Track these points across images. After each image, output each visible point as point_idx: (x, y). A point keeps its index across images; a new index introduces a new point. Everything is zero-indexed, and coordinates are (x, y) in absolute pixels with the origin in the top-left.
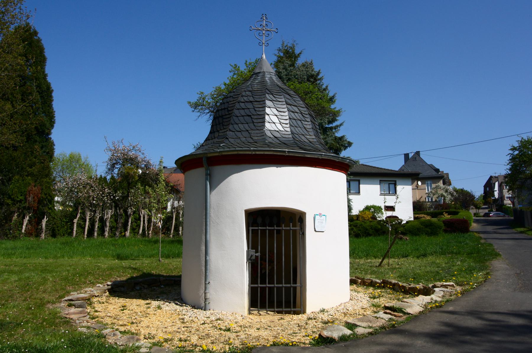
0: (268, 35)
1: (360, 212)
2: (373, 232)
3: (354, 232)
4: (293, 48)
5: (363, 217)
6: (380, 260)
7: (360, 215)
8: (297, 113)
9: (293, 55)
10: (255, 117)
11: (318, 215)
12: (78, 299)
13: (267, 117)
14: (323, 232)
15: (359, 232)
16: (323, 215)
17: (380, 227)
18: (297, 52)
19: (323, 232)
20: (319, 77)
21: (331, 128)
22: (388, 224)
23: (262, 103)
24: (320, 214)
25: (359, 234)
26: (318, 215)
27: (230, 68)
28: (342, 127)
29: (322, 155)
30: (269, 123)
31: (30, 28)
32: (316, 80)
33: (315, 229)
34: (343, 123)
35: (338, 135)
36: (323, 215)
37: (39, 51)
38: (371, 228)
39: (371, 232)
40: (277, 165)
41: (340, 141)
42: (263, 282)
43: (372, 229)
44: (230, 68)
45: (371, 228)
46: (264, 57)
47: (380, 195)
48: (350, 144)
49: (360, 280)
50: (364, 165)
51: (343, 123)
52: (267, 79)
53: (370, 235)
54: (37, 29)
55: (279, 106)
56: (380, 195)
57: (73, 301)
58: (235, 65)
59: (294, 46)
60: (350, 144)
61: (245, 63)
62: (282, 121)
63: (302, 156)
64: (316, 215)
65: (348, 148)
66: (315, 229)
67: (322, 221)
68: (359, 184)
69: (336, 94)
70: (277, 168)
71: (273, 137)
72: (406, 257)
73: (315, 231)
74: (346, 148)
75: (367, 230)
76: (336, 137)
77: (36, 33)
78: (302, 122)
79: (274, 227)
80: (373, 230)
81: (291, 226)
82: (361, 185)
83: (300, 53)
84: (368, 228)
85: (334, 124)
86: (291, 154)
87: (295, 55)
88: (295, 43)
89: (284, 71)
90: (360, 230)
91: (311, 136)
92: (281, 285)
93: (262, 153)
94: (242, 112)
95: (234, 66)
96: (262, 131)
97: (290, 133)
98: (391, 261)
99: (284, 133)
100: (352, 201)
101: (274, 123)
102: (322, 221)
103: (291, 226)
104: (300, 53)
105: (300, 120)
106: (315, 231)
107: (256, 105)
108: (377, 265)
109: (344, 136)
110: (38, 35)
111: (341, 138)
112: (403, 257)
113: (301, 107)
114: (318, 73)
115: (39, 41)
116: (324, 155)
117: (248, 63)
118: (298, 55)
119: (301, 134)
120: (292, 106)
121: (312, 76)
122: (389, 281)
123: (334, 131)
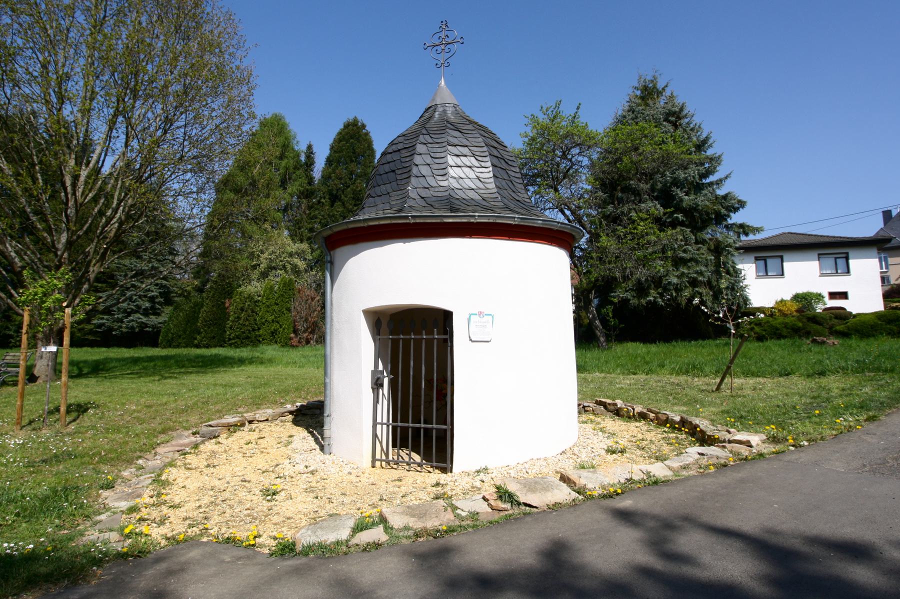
1: (776, 302)
5: (779, 310)
6: (718, 380)
8: (466, 156)
9: (655, 90)
10: (400, 172)
13: (415, 170)
17: (800, 325)
18: (660, 86)
20: (685, 112)
21: (711, 184)
23: (411, 149)
24: (480, 313)
25: (764, 336)
27: (526, 121)
31: (358, 122)
32: (679, 118)
34: (730, 174)
35: (721, 192)
37: (366, 145)
38: (785, 327)
42: (405, 419)
44: (526, 121)
45: (785, 327)
48: (742, 204)
49: (654, 415)
50: (792, 233)
51: (730, 174)
53: (785, 337)
54: (365, 123)
55: (435, 150)
60: (742, 204)
62: (435, 172)
63: (439, 221)
65: (741, 209)
68: (782, 262)
72: (787, 375)
73: (471, 340)
74: (736, 210)
75: (777, 329)
76: (717, 197)
77: (364, 126)
78: (474, 169)
82: (785, 264)
84: (778, 326)
85: (712, 179)
86: (418, 221)
90: (765, 330)
92: (406, 425)
93: (376, 223)
94: (387, 168)
96: (404, 191)
97: (495, 190)
98: (738, 382)
104: (666, 86)
105: (470, 167)
106: (471, 340)
107: (405, 153)
108: (714, 389)
109: (729, 193)
111: (725, 197)
112: (781, 376)
114: (681, 109)
115: (367, 134)
116: (479, 216)
117: (544, 109)
118: (663, 89)
119: (467, 187)
121: (674, 114)
123: (715, 187)
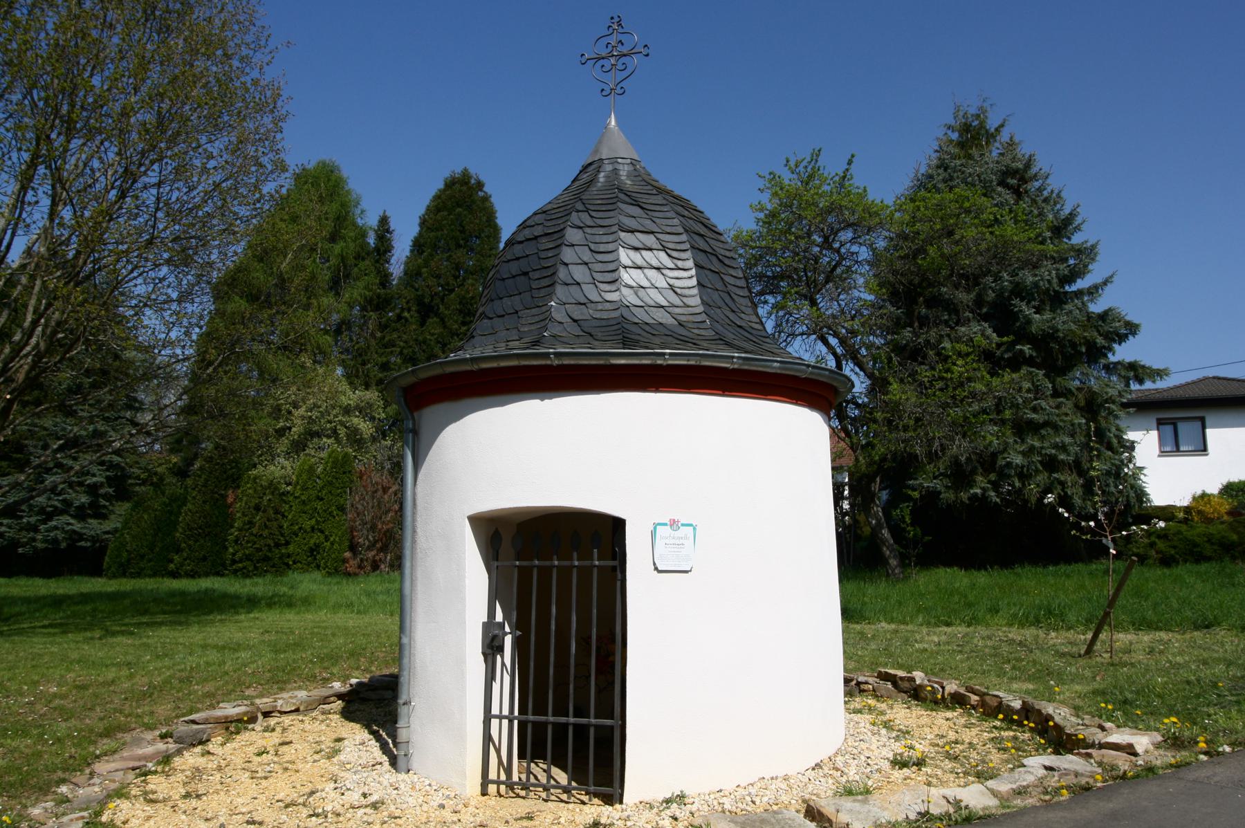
0: (623, 67)
1: (1194, 498)
2: (1215, 551)
3: (1157, 552)
4: (980, 115)
5: (1200, 512)
6: (1089, 636)
7: (1193, 508)
8: (650, 249)
9: (983, 132)
10: (536, 275)
11: (665, 524)
12: (207, 719)
13: (562, 273)
14: (686, 572)
15: (1173, 552)
16: (683, 525)
17: (1235, 537)
18: (992, 124)
19: (686, 572)
20: (1034, 170)
21: (1079, 294)
22: (1106, 537)
23: (556, 236)
24: (673, 523)
25: (1172, 556)
26: (665, 524)
27: (761, 184)
28: (1108, 289)
29: (733, 357)
30: (567, 285)
31: (470, 177)
32: (1024, 180)
33: (654, 564)
34: (1112, 277)
35: (1096, 308)
36: (683, 525)
37: (484, 219)
38: (1209, 541)
39: (1208, 550)
40: (541, 395)
41: (1100, 323)
42: (540, 709)
43: (1212, 544)
44: (761, 184)
45: (1209, 541)
46: (613, 123)
47: (1159, 456)
48: (1132, 329)
49: (977, 698)
50: (1219, 378)
51: (1112, 277)
52: (623, 178)
53: (1208, 559)
54: (482, 178)
55: (597, 239)
56: (1159, 456)
57: (198, 724)
58: (770, 174)
59: (984, 112)
60: (1132, 329)
61: (786, 165)
62: (598, 276)
63: (601, 362)
64: (659, 524)
65: (1131, 337)
66: (654, 564)
67: (681, 541)
68: (1204, 428)
69: (1078, 206)
70: (542, 400)
71: (569, 320)
72: (1207, 627)
73: (656, 569)
74: (1122, 338)
75: (1196, 545)
76: (1089, 316)
77: (480, 185)
78: (665, 271)
79: (571, 559)
80: (1216, 547)
81: (596, 556)
82: (1209, 432)
83: (1002, 126)
84: (1197, 540)
85: (1081, 284)
86: (566, 362)
87: (987, 131)
88: (985, 105)
89: (941, 171)
90: (1175, 547)
91: (688, 306)
92: (543, 718)
93: (495, 365)
94: (514, 268)
95: (767, 177)
96: (544, 309)
97: (701, 309)
98: (1123, 638)
99: (600, 307)
100: (1145, 471)
101: (578, 284)
102: (681, 541)
103: (596, 556)
104: (1002, 126)
105: (658, 269)
106: (656, 569)
107: (545, 243)
108: (1082, 652)
109: (1110, 310)
110: (484, 189)
111: (1104, 316)
112: (1197, 627)
113: (669, 233)
114: (1028, 165)
115: (486, 198)
116: (671, 354)
117: (792, 164)
118: (997, 130)
119: (653, 304)
120: (638, 234)
121: (1013, 173)
122: (1037, 707)
123: (1086, 298)
